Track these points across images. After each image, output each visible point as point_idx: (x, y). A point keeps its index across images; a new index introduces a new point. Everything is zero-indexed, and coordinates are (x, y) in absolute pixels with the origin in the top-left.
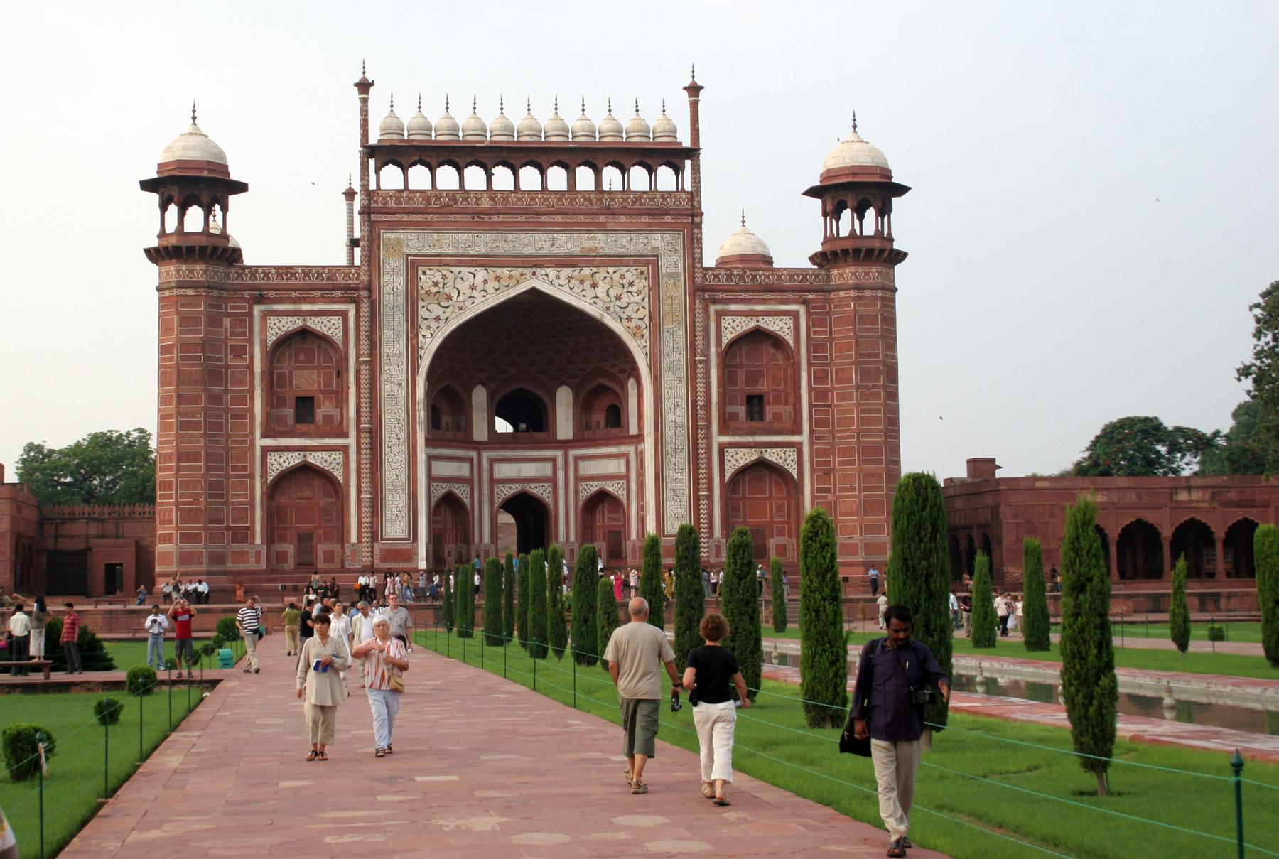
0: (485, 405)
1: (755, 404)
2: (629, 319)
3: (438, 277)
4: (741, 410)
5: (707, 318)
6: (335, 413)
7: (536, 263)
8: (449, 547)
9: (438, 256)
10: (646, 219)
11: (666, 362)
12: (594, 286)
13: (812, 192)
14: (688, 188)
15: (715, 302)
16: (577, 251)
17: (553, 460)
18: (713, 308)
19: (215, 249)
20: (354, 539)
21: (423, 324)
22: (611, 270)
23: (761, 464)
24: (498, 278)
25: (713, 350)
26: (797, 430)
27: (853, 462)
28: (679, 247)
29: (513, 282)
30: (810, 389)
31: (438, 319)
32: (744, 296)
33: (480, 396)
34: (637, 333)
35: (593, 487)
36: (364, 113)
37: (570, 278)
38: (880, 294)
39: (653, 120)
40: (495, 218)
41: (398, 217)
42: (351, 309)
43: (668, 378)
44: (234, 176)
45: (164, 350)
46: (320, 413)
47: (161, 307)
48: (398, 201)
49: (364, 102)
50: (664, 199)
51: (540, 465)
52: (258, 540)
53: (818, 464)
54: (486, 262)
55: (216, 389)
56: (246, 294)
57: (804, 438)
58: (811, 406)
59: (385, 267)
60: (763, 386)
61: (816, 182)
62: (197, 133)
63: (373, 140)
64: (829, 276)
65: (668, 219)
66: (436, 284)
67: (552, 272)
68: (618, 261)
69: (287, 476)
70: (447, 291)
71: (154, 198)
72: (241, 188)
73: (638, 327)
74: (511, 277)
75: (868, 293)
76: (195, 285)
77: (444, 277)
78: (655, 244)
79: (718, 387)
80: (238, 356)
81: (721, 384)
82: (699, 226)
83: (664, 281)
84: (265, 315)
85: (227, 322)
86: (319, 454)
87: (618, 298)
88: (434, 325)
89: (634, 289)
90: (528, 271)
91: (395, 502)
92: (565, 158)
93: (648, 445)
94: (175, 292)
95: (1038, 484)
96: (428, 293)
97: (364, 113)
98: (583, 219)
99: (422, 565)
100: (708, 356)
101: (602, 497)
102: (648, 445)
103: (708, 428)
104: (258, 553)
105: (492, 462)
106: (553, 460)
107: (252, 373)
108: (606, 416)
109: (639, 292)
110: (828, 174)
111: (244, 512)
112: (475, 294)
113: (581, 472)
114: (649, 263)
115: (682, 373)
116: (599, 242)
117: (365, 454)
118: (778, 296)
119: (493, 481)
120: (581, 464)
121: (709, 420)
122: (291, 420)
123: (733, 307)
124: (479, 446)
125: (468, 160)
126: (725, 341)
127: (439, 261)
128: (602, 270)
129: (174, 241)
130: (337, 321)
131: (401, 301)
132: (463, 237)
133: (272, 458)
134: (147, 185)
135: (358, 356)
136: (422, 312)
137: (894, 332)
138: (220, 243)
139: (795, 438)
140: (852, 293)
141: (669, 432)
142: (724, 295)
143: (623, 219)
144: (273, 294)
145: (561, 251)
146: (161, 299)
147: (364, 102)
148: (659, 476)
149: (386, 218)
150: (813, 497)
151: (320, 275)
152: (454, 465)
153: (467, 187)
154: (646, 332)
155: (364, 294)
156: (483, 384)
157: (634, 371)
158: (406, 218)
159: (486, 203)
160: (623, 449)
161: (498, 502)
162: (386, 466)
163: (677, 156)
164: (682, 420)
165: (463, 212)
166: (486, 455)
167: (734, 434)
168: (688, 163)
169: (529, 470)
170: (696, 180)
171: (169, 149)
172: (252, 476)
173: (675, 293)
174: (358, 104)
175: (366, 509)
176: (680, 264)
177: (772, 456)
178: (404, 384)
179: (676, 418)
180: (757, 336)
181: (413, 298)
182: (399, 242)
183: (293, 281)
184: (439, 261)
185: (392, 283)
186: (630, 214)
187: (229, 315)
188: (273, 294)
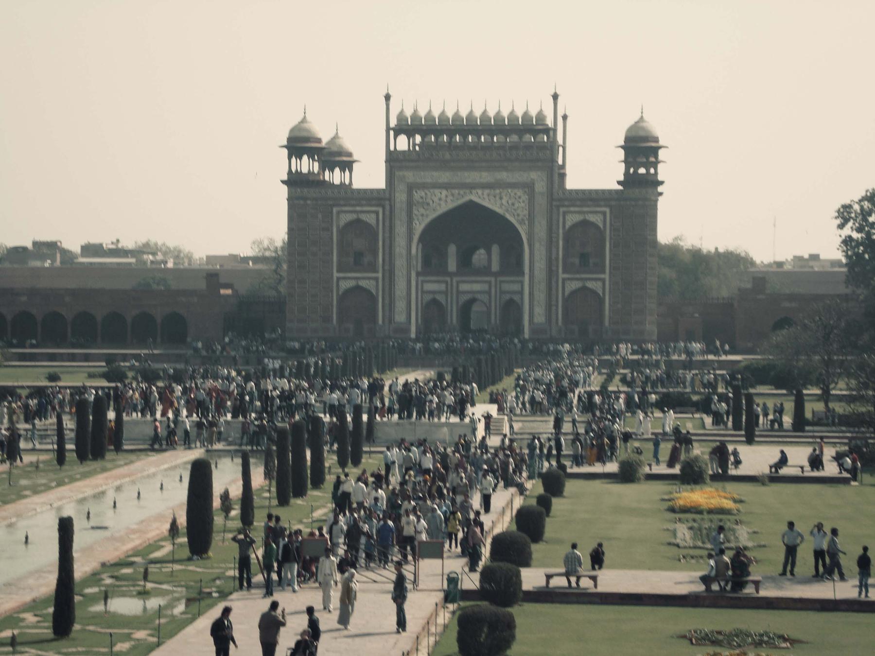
0: (455, 252)
1: (584, 257)
2: (518, 215)
3: (423, 194)
4: (577, 261)
5: (558, 214)
7: (472, 187)
9: (424, 183)
12: (501, 198)
15: (563, 206)
16: (492, 180)
18: (562, 210)
19: (313, 182)
20: (380, 322)
25: (561, 231)
26: (604, 272)
28: (545, 179)
31: (422, 215)
33: (452, 249)
34: (521, 222)
35: (508, 297)
37: (488, 195)
39: (533, 113)
42: (380, 210)
43: (537, 245)
54: (447, 186)
57: (607, 276)
62: (304, 120)
65: (540, 164)
66: (422, 198)
67: (480, 192)
68: (513, 186)
69: (349, 292)
73: (523, 220)
74: (459, 194)
75: (640, 203)
76: (305, 199)
81: (565, 249)
85: (320, 216)
87: (513, 204)
88: (420, 218)
89: (521, 201)
90: (468, 191)
93: (527, 278)
96: (418, 202)
99: (413, 336)
100: (558, 235)
102: (527, 278)
105: (458, 283)
106: (490, 283)
108: (513, 263)
110: (628, 139)
114: (529, 187)
116: (503, 176)
117: (387, 280)
119: (458, 292)
121: (557, 267)
123: (572, 209)
126: (567, 227)
127: (424, 186)
128: (505, 191)
130: (374, 216)
131: (404, 206)
132: (436, 174)
135: (384, 232)
136: (415, 212)
138: (317, 178)
139: (602, 276)
140: (633, 203)
141: (536, 273)
148: (531, 294)
150: (610, 305)
154: (527, 222)
155: (387, 202)
160: (520, 278)
161: (460, 303)
163: (547, 131)
166: (455, 279)
168: (551, 133)
169: (476, 287)
171: (292, 131)
172: (332, 291)
173: (541, 202)
175: (387, 308)
177: (590, 285)
179: (540, 265)
180: (585, 223)
181: (410, 204)
184: (424, 186)
185: (401, 197)
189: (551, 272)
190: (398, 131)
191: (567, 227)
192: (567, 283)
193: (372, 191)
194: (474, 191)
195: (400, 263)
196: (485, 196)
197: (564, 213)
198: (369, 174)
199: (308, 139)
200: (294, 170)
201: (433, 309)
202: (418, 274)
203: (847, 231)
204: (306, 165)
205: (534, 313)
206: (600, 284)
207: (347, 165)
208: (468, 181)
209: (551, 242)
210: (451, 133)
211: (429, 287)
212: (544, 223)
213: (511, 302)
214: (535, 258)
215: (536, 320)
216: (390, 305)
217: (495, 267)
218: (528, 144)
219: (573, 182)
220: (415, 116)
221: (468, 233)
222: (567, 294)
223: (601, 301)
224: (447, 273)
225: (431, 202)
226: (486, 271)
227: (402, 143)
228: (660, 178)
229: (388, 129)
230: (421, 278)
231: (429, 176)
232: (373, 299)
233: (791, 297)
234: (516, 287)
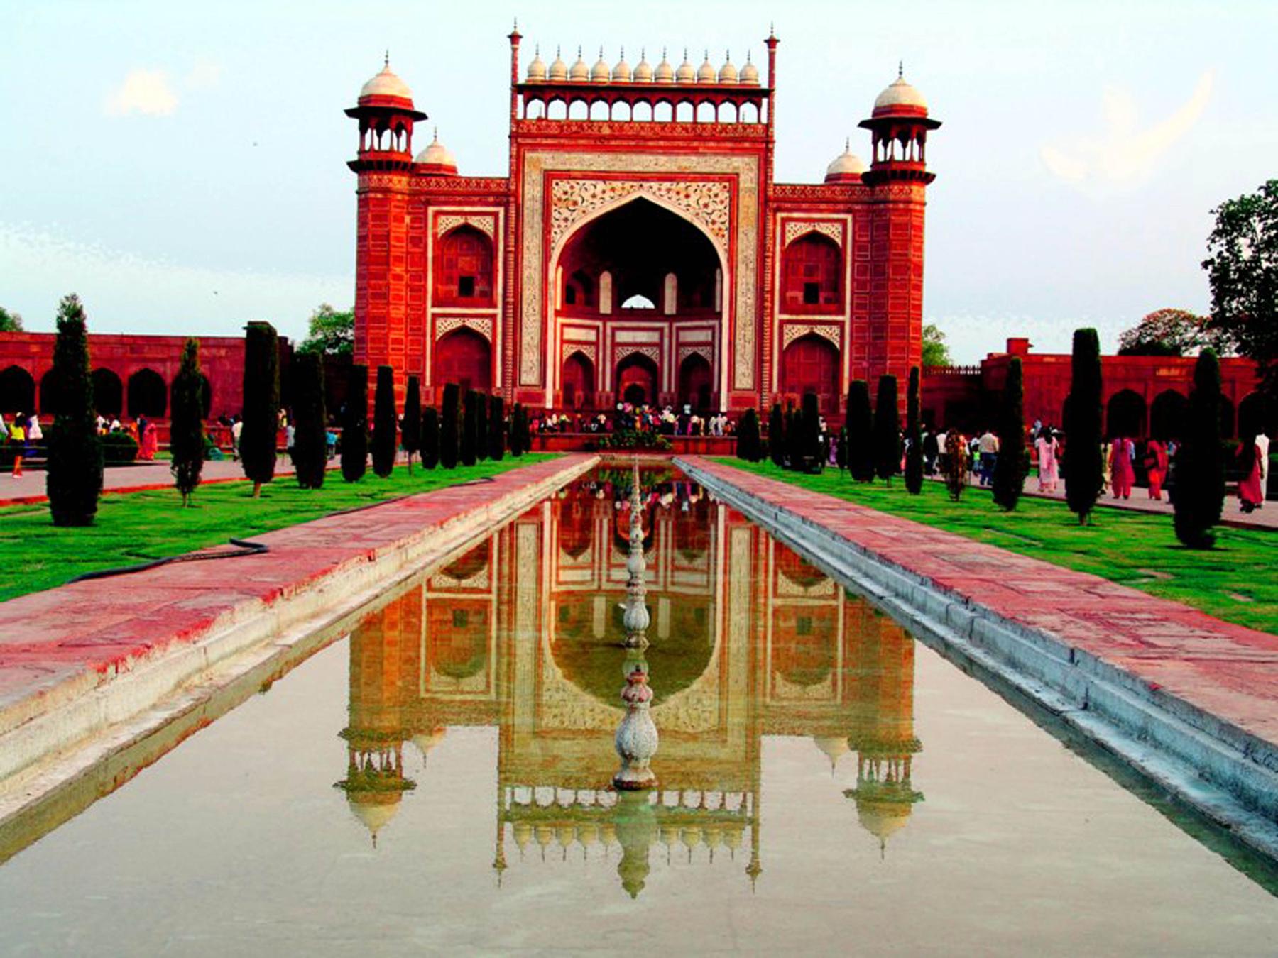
1: (811, 294)
2: (714, 222)
3: (567, 188)
4: (800, 295)
5: (775, 223)
6: (486, 289)
7: (642, 177)
8: (579, 394)
10: (729, 145)
11: (740, 257)
12: (687, 196)
13: (864, 124)
14: (764, 120)
16: (675, 169)
17: (661, 330)
18: (780, 215)
19: (398, 163)
20: (499, 384)
21: (555, 223)
22: (701, 184)
23: (812, 338)
24: (613, 190)
25: (778, 248)
26: (843, 313)
27: (882, 338)
28: (755, 167)
29: (624, 193)
30: (853, 279)
31: (566, 220)
32: (805, 206)
33: (606, 280)
35: (688, 351)
36: (514, 58)
37: (669, 190)
38: (912, 206)
40: (613, 143)
41: (538, 141)
42: (501, 210)
43: (741, 269)
44: (418, 108)
45: (361, 239)
46: (478, 289)
47: (360, 207)
48: (539, 128)
49: (515, 50)
50: (745, 129)
51: (651, 333)
52: (428, 383)
53: (857, 338)
55: (398, 270)
56: (423, 198)
57: (846, 318)
58: (853, 293)
59: (527, 179)
60: (819, 277)
61: (868, 116)
63: (522, 80)
64: (873, 192)
65: (747, 145)
66: (565, 193)
67: (655, 185)
68: (705, 177)
70: (575, 198)
71: (356, 122)
72: (422, 117)
76: (386, 191)
77: (572, 187)
78: (736, 164)
79: (781, 275)
80: (415, 245)
82: (771, 151)
83: (741, 194)
84: (437, 214)
85: (408, 219)
86: (476, 320)
87: (706, 206)
88: (563, 224)
89: (718, 200)
90: (636, 184)
91: (530, 358)
92: (669, 96)
94: (372, 195)
95: (1047, 360)
96: (559, 199)
97: (514, 58)
98: (681, 144)
99: (549, 405)
100: (774, 253)
103: (772, 308)
104: (427, 393)
105: (614, 330)
107: (426, 258)
108: (700, 299)
109: (722, 202)
111: (417, 362)
112: (595, 200)
113: (681, 339)
114: (732, 180)
115: (751, 266)
118: (831, 206)
119: (615, 345)
120: (682, 334)
121: (772, 302)
122: (455, 294)
123: (796, 215)
124: (605, 318)
125: (593, 96)
126: (788, 241)
127: (567, 175)
128: (694, 185)
129: (368, 157)
130: (490, 219)
131: (538, 206)
132: (588, 157)
133: (439, 322)
134: (350, 113)
135: (506, 246)
136: (555, 214)
137: (921, 237)
138: (406, 159)
139: (839, 318)
140: (891, 206)
141: (740, 311)
142: (788, 205)
143: (712, 144)
144: (442, 198)
145: (663, 169)
146: (360, 201)
147: (515, 50)
149: (529, 141)
151: (478, 184)
152: (583, 331)
153: (592, 118)
154: (726, 233)
156: (610, 271)
157: (718, 264)
158: (544, 141)
159: (606, 131)
160: (711, 323)
161: (617, 360)
162: (524, 330)
164: (751, 302)
165: (588, 137)
166: (609, 324)
167: (791, 313)
168: (765, 101)
169: (642, 337)
170: (770, 115)
172: (424, 335)
173: (749, 204)
174: (510, 52)
176: (755, 180)
177: (821, 331)
178: (539, 269)
179: (746, 300)
180: (814, 239)
182: (538, 160)
183: (458, 188)
184: (567, 175)
185: (532, 191)
186: (718, 140)
187: (409, 213)
188: (442, 198)
191: (788, 241)
192: (787, 328)
193: (488, 181)
194: (646, 185)
195: (530, 293)
196: (663, 193)
197: (784, 221)
200: (367, 148)
201: (579, 368)
202: (557, 313)
206: (836, 329)
208: (636, 169)
211: (571, 334)
212: (753, 236)
214: (738, 288)
215: (738, 385)
216: (514, 356)
217: (670, 307)
222: (785, 345)
223: (837, 355)
224: (596, 315)
225: (580, 200)
228: (928, 169)
229: (517, 89)
230: (560, 320)
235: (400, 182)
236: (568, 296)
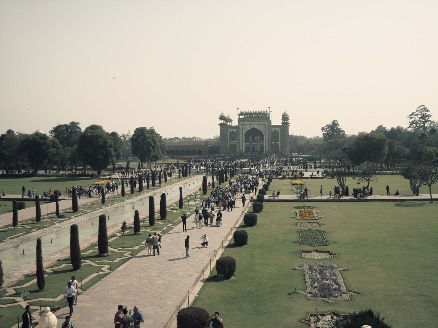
1: (275, 137)
7: (254, 125)
33: (250, 136)
54: (249, 125)
68: (262, 124)
91: (241, 147)
101: (262, 146)
108: (262, 139)
114: (265, 125)
116: (260, 123)
127: (245, 125)
163: (268, 114)
173: (267, 127)
179: (267, 139)
181: (242, 128)
184: (245, 125)
185: (241, 127)
189: (269, 141)
190: (240, 115)
195: (241, 139)
198: (235, 123)
199: (223, 117)
201: (247, 148)
203: (323, 132)
204: (223, 122)
205: (266, 148)
207: (231, 121)
209: (269, 135)
210: (250, 115)
213: (262, 146)
214: (266, 138)
217: (259, 140)
218: (264, 117)
219: (273, 124)
220: (243, 112)
221: (253, 134)
223: (279, 146)
226: (257, 140)
227: (241, 117)
231: (246, 123)
232: (236, 146)
233: (314, 144)
234: (263, 143)
235: (224, 126)
236: (246, 138)
